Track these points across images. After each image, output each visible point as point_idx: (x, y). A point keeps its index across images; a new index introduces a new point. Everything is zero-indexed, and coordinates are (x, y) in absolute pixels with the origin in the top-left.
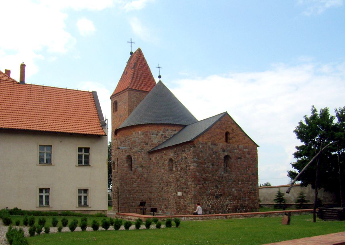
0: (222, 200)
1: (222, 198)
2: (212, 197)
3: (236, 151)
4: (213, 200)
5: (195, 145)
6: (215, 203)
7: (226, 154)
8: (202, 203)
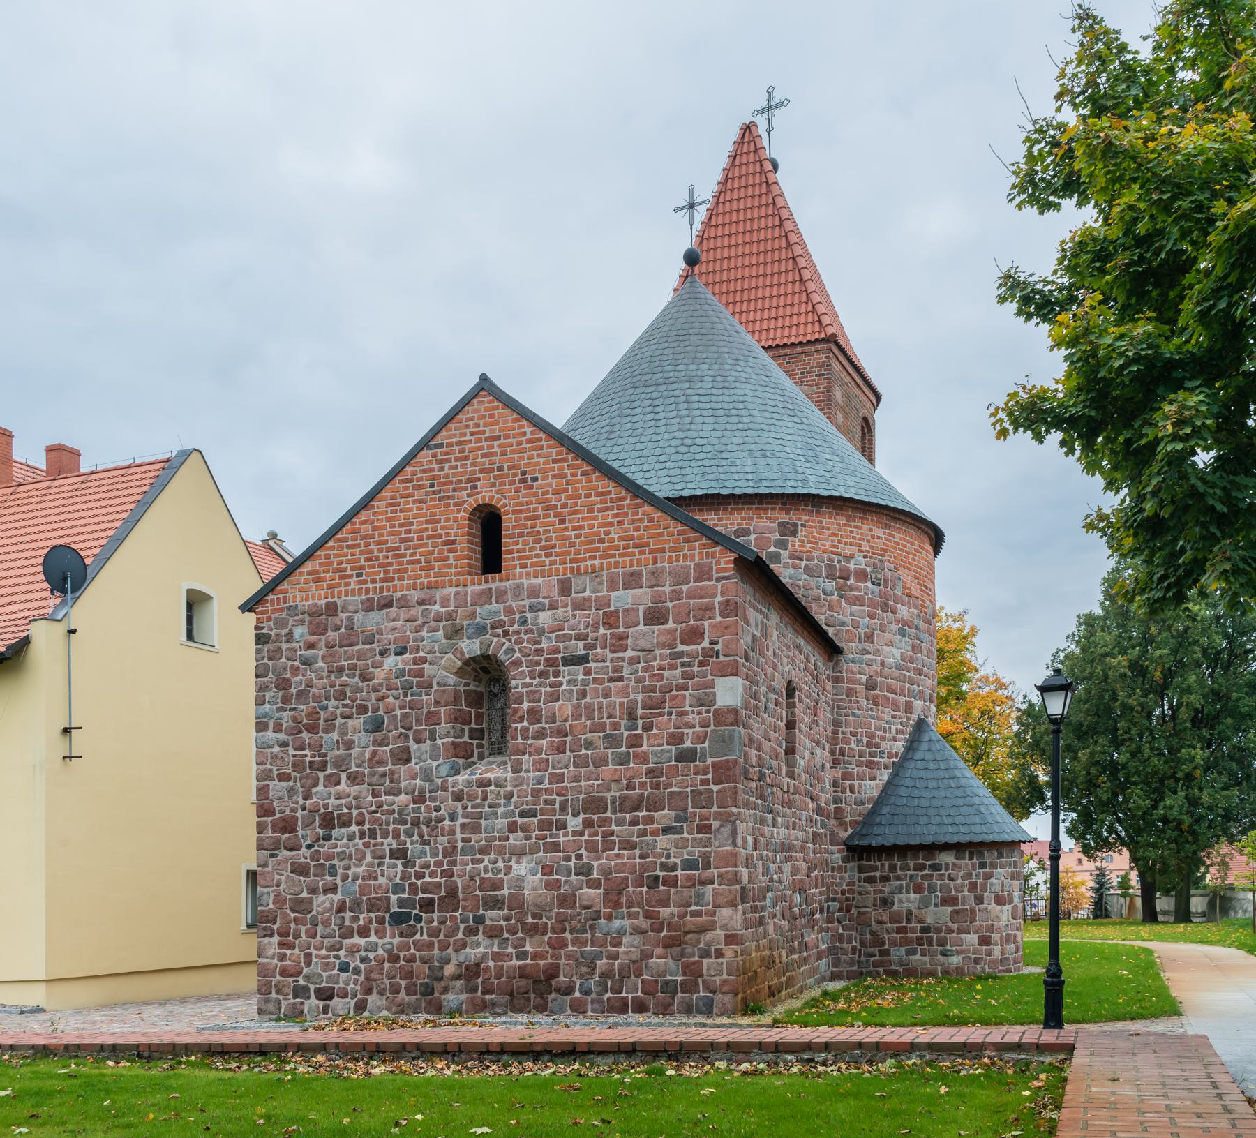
0: (442, 937)
1: (435, 924)
2: (373, 915)
3: (545, 617)
4: (380, 934)
5: (265, 631)
6: (389, 952)
7: (471, 647)
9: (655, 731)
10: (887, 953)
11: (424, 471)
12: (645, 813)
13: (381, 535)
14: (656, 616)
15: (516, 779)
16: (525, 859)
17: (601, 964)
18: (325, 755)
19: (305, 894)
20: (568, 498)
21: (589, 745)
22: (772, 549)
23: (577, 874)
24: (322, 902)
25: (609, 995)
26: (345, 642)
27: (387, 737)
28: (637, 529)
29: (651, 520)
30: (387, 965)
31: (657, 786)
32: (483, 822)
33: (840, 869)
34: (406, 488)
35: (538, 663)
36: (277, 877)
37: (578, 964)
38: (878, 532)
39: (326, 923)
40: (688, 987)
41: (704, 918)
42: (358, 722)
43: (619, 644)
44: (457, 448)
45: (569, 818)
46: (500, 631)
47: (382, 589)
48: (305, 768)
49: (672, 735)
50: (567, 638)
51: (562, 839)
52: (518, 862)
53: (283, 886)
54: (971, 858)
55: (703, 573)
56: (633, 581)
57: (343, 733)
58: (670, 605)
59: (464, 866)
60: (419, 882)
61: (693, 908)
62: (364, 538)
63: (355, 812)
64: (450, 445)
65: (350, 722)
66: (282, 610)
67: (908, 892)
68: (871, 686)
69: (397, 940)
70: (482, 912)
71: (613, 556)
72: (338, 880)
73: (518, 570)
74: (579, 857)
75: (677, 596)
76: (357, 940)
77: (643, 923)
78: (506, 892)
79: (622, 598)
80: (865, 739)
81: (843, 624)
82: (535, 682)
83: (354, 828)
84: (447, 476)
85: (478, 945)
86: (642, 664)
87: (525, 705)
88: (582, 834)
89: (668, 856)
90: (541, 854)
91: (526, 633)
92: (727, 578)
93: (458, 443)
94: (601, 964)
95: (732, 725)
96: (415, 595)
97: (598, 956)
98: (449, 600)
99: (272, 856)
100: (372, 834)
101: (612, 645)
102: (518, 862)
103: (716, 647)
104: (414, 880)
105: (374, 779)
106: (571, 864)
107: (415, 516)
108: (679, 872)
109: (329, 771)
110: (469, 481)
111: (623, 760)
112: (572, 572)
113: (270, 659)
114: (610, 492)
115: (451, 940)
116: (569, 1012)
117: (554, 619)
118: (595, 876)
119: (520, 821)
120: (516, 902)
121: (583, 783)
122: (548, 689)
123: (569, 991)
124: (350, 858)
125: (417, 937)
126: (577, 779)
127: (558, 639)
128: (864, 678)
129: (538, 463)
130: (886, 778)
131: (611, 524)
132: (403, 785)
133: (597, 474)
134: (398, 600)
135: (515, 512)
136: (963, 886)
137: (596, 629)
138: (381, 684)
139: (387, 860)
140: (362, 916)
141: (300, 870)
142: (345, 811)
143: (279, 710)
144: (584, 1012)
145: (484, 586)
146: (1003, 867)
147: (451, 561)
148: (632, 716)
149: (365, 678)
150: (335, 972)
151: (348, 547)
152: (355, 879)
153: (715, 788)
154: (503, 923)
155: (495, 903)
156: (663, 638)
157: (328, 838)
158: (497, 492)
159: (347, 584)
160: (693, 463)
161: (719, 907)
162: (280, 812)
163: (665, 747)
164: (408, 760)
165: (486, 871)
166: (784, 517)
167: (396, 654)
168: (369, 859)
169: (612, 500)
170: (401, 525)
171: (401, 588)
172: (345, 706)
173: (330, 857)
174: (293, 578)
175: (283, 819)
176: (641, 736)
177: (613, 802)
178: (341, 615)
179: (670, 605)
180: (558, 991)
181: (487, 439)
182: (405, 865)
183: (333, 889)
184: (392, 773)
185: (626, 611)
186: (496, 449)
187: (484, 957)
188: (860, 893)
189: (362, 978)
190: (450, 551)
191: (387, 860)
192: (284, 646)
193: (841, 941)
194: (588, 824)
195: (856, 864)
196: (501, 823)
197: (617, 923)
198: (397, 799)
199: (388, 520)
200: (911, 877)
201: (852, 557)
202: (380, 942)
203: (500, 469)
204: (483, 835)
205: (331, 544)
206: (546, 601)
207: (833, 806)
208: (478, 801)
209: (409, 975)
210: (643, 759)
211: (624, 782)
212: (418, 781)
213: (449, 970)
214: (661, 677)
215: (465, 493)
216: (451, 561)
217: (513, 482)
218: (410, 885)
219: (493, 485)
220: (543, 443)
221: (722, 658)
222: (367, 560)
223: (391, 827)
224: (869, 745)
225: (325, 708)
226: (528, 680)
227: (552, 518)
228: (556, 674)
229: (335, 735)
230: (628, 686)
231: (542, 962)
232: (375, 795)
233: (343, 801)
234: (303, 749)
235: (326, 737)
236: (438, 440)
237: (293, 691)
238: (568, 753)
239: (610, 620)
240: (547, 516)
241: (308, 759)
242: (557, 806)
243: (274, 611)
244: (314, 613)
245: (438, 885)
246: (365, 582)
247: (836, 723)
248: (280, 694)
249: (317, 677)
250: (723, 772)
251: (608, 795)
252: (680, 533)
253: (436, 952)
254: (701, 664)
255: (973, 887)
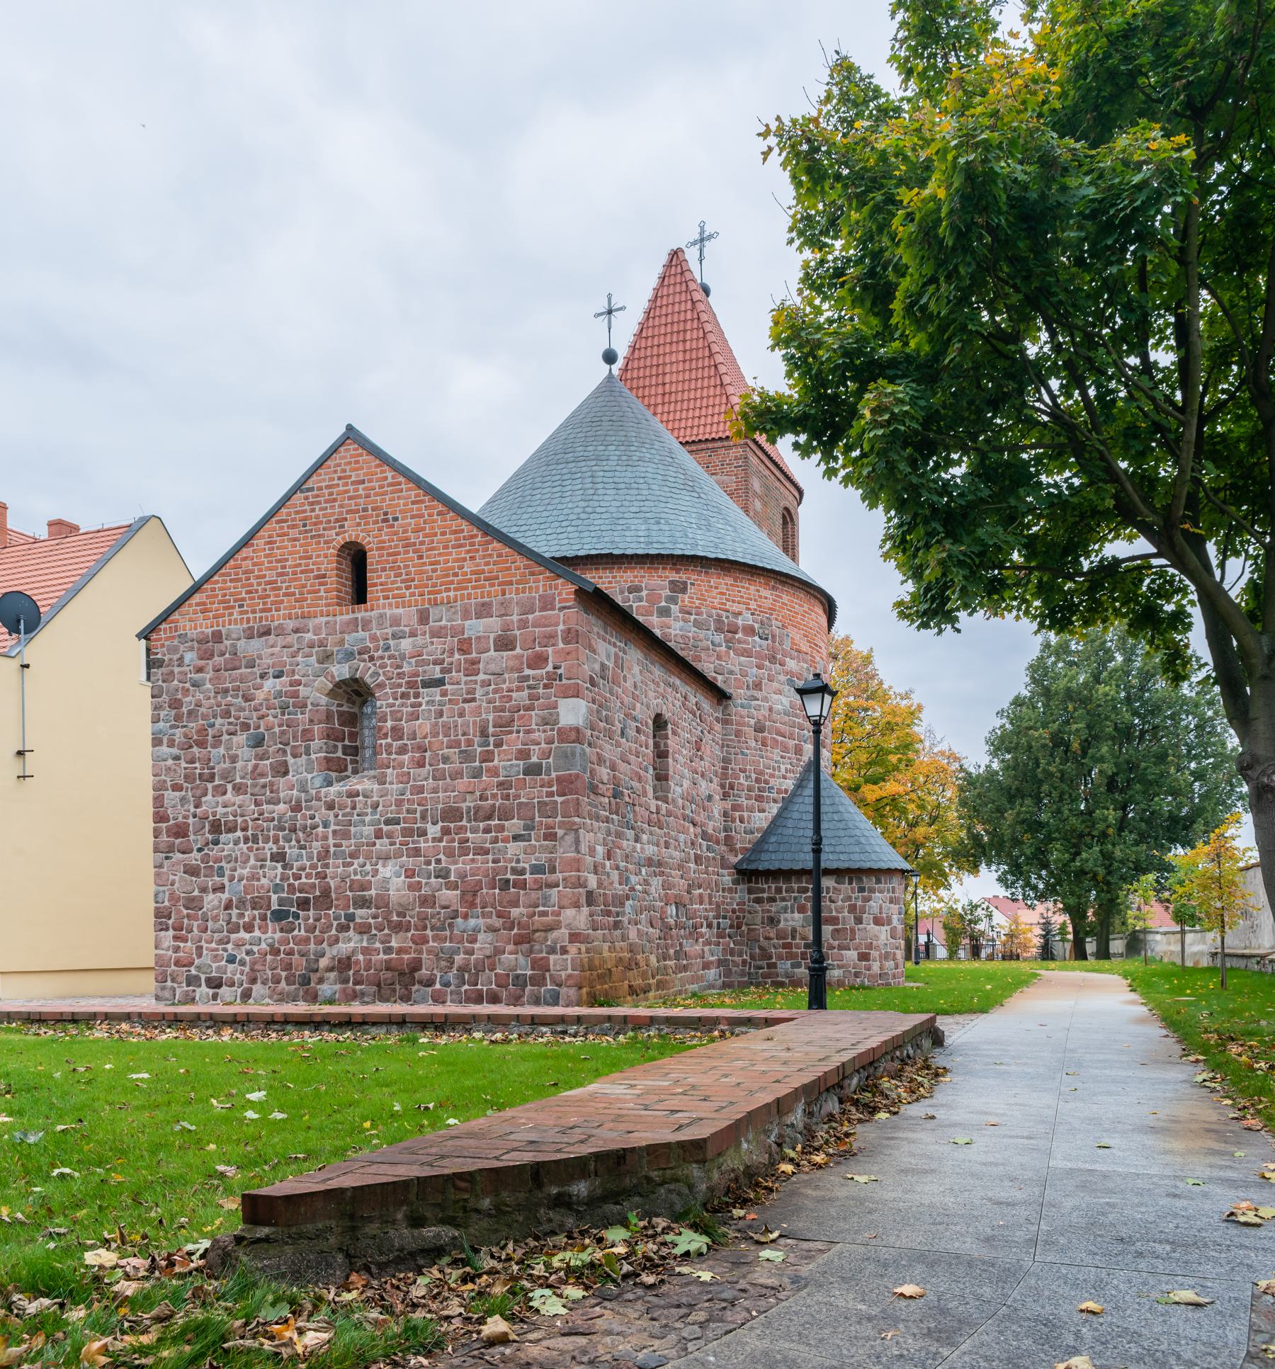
0: (317, 933)
1: (311, 921)
2: (256, 912)
3: (406, 644)
4: (264, 929)
5: (159, 656)
6: (271, 946)
7: (341, 671)
8: (200, 948)
9: (505, 747)
10: (774, 966)
11: (297, 513)
12: (497, 822)
13: (260, 570)
14: (505, 643)
15: (381, 790)
16: (390, 862)
17: (459, 959)
18: (213, 768)
19: (196, 893)
20: (426, 536)
21: (446, 759)
22: (663, 604)
23: (436, 877)
24: (211, 900)
25: (466, 987)
26: (229, 666)
27: (267, 752)
28: (487, 564)
29: (500, 555)
30: (269, 957)
31: (507, 797)
32: (352, 829)
33: (730, 890)
34: (282, 528)
35: (400, 686)
36: (171, 877)
37: (439, 959)
38: (766, 593)
39: (216, 919)
40: (538, 981)
41: (550, 918)
42: (241, 738)
43: (472, 668)
44: (326, 491)
45: (429, 825)
46: (366, 657)
47: (261, 618)
48: (195, 779)
49: (520, 751)
50: (427, 663)
51: (422, 845)
52: (384, 866)
53: (177, 885)
54: (850, 883)
55: (547, 604)
56: (484, 610)
57: (228, 749)
58: (517, 633)
59: (335, 868)
60: (296, 883)
61: (541, 908)
62: (245, 572)
63: (240, 820)
64: (320, 489)
65: (235, 738)
66: (173, 637)
67: (793, 912)
68: (759, 729)
69: (278, 935)
70: (352, 910)
71: (466, 588)
72: (225, 881)
73: (382, 601)
74: (438, 861)
75: (523, 624)
76: (243, 935)
77: (497, 922)
78: (373, 892)
79: (475, 627)
80: (754, 776)
81: (731, 672)
82: (397, 703)
83: (239, 834)
84: (317, 517)
85: (350, 940)
86: (493, 686)
87: (389, 724)
88: (440, 840)
89: (518, 861)
90: (404, 858)
91: (389, 658)
92: (569, 608)
93: (327, 487)
94: (459, 959)
95: (573, 742)
96: (291, 624)
97: (457, 952)
98: (320, 628)
99: (167, 858)
100: (255, 840)
101: (466, 669)
102: (384, 866)
103: (559, 671)
104: (291, 881)
105: (256, 790)
106: (431, 867)
107: (291, 553)
108: (527, 876)
109: (217, 783)
110: (337, 521)
111: (477, 774)
112: (429, 603)
113: (164, 681)
114: (463, 531)
115: (326, 936)
116: (431, 1002)
117: (414, 646)
118: (452, 878)
119: (385, 828)
120: (382, 903)
121: (441, 794)
122: (410, 709)
123: (429, 983)
124: (236, 861)
125: (296, 932)
126: (435, 791)
127: (418, 664)
128: (752, 722)
129: (398, 505)
130: (775, 811)
131: (464, 560)
132: (282, 795)
133: (452, 514)
134: (276, 628)
135: (378, 549)
136: (843, 908)
137: (451, 654)
138: (261, 704)
139: (268, 863)
140: (246, 913)
141: (192, 871)
142: (231, 818)
143: (172, 727)
144: (444, 1002)
145: (351, 616)
146: (881, 892)
147: (322, 593)
148: (484, 733)
149: (247, 699)
150: (223, 963)
151: (231, 581)
152: (240, 880)
153: (559, 799)
154: (371, 921)
155: (364, 903)
156: (511, 663)
157: (216, 842)
158: (362, 531)
159: (230, 615)
160: (592, 528)
161: (563, 907)
162: (175, 819)
163: (514, 762)
164: (286, 773)
165: (356, 873)
166: (674, 576)
167: (275, 677)
168: (252, 861)
169: (464, 538)
170: (278, 561)
171: (278, 618)
172: (230, 724)
173: (218, 860)
174: (184, 609)
175: (177, 825)
176: (493, 752)
177: (468, 812)
178: (226, 642)
179: (517, 633)
180: (420, 982)
181: (353, 483)
182: (284, 867)
183: (221, 888)
184: (272, 784)
185: (478, 638)
186: (361, 492)
187: (354, 952)
188: (750, 912)
189: (247, 969)
190: (321, 584)
191: (268, 863)
192: (176, 670)
193: (732, 954)
194: (446, 831)
195: (746, 886)
196: (368, 830)
197: (472, 922)
198: (276, 808)
199: (266, 556)
200: (795, 898)
201: (740, 613)
202: (263, 937)
203: (365, 510)
204: (353, 841)
205: (216, 578)
206: (407, 629)
207: (723, 834)
208: (348, 810)
209: (288, 967)
210: (494, 772)
211: (478, 794)
212: (295, 792)
213: (323, 963)
214: (510, 698)
215: (333, 532)
216: (322, 593)
217: (377, 522)
218: (289, 885)
219: (359, 524)
220: (403, 486)
221: (564, 681)
222: (248, 592)
223: (272, 833)
224: (758, 781)
225: (213, 725)
226: (391, 701)
227: (411, 554)
228: (417, 696)
229: (222, 750)
230: (480, 706)
231: (406, 957)
232: (257, 804)
233: (229, 809)
234: (194, 762)
235: (214, 751)
236: (310, 484)
237: (185, 710)
238: (427, 766)
239: (465, 646)
240: (407, 552)
241: (198, 771)
242: (418, 815)
243: (167, 639)
244: (202, 641)
245: (313, 886)
246: (247, 612)
247: (726, 760)
248: (173, 712)
249: (203, 697)
250: (566, 785)
251: (464, 806)
252: (526, 567)
253: (312, 946)
254: (546, 686)
255: (852, 909)
